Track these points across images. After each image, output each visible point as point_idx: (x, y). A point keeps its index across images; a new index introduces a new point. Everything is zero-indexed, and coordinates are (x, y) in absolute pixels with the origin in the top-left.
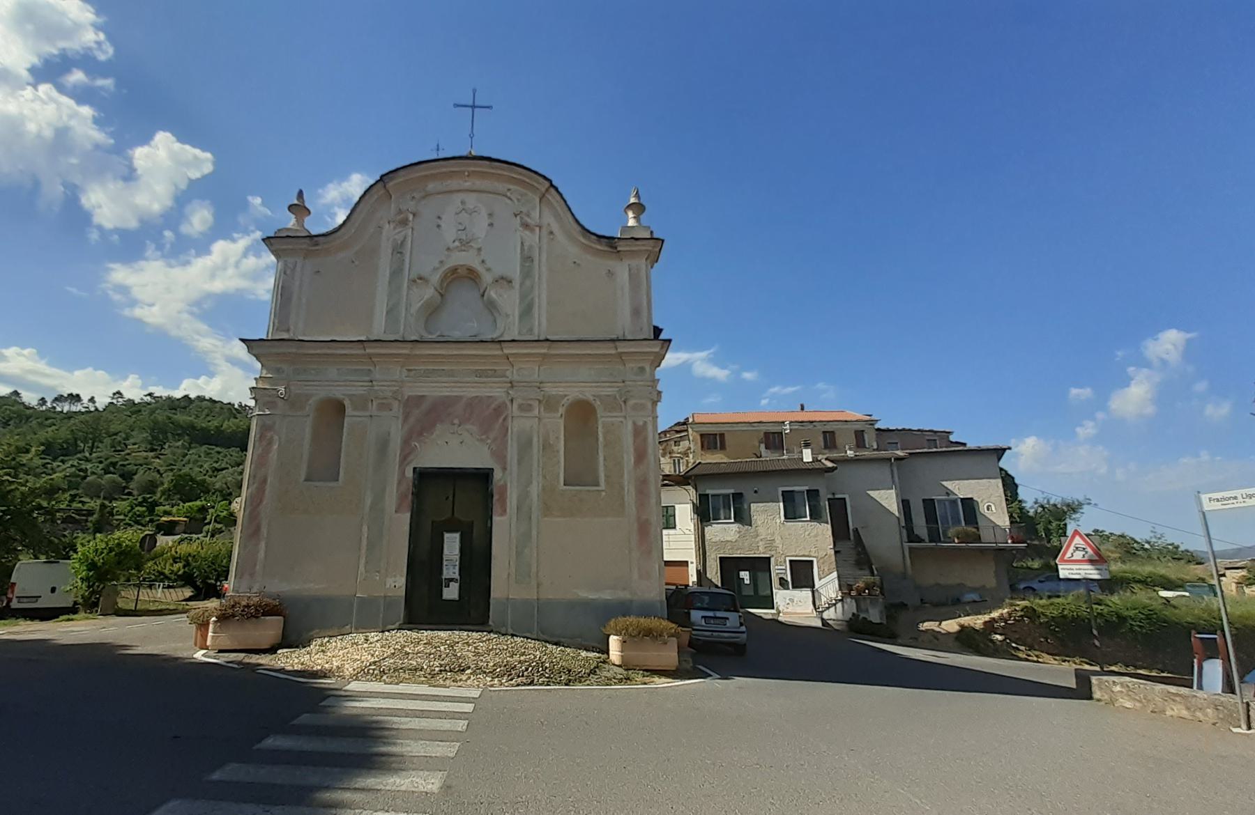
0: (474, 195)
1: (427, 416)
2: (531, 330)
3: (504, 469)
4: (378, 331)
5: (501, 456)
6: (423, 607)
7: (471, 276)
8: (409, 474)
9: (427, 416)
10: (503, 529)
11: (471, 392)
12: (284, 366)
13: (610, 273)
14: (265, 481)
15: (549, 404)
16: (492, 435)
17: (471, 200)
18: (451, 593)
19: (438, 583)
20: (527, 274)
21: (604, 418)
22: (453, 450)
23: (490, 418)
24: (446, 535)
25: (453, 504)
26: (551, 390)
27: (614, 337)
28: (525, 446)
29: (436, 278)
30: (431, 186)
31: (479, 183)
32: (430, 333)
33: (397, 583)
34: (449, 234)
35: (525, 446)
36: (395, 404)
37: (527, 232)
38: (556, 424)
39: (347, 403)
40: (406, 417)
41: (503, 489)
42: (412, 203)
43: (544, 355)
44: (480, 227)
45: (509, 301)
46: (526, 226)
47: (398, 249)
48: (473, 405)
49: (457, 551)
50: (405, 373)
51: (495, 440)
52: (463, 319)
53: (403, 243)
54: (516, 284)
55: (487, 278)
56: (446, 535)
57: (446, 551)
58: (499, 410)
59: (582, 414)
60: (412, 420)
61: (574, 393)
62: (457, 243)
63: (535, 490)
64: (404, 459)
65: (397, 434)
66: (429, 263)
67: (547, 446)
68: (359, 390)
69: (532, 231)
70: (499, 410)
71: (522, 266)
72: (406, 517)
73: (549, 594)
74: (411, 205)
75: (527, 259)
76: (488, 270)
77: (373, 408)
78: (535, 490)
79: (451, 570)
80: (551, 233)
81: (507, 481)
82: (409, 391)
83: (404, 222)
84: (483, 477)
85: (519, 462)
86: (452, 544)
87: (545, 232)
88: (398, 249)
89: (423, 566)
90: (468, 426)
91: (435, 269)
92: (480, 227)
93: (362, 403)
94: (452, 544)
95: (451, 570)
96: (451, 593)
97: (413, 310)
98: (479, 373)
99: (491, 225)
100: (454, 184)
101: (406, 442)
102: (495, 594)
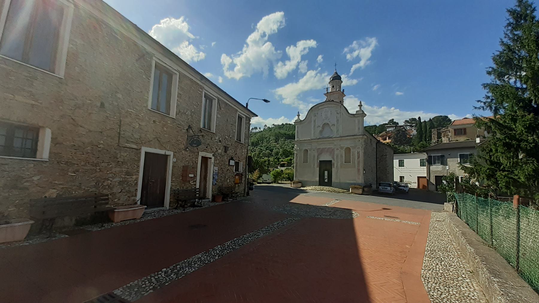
1: (321, 152)
4: (313, 138)
6: (322, 183)
7: (328, 124)
9: (321, 152)
10: (334, 170)
15: (342, 148)
18: (326, 181)
19: (324, 179)
20: (338, 123)
21: (352, 150)
22: (326, 157)
25: (326, 166)
26: (342, 146)
28: (337, 156)
30: (320, 108)
33: (318, 179)
35: (337, 156)
45: (334, 129)
47: (315, 121)
55: (330, 125)
58: (333, 150)
59: (348, 150)
61: (346, 146)
67: (341, 156)
68: (310, 148)
70: (333, 150)
72: (318, 169)
73: (342, 181)
75: (338, 120)
79: (326, 177)
84: (331, 161)
86: (326, 173)
88: (315, 121)
89: (321, 176)
94: (326, 173)
95: (326, 177)
96: (326, 181)
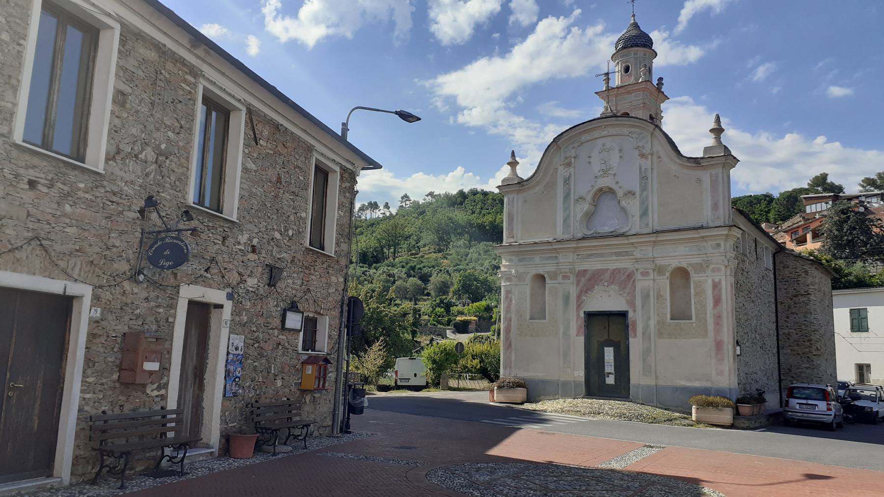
0: (610, 139)
1: (590, 281)
2: (647, 225)
3: (635, 311)
4: (560, 235)
5: (632, 303)
6: (595, 387)
7: (611, 191)
8: (582, 315)
9: (590, 281)
10: (635, 345)
11: (613, 266)
12: (514, 258)
13: (699, 181)
14: (510, 320)
15: (660, 270)
16: (627, 291)
17: (609, 142)
18: (610, 380)
19: (602, 375)
20: (644, 189)
21: (694, 277)
22: (606, 301)
23: (624, 280)
24: (606, 349)
25: (607, 330)
26: (660, 262)
27: (699, 225)
28: (646, 297)
29: (589, 197)
30: (584, 138)
31: (613, 131)
32: (590, 230)
33: (580, 374)
34: (596, 167)
35: (646, 297)
36: (571, 276)
37: (643, 160)
38: (664, 283)
39: (546, 276)
40: (578, 284)
41: (634, 324)
42: (573, 151)
43: (655, 242)
44: (614, 160)
45: (633, 206)
46: (642, 155)
47: (567, 181)
48: (615, 272)
49: (612, 358)
50: (576, 257)
51: (629, 293)
52: (607, 223)
53: (569, 178)
54: (638, 194)
55: (620, 193)
56: (606, 349)
57: (606, 358)
58: (630, 276)
59: (681, 275)
60: (581, 284)
61: (675, 263)
62: (601, 173)
63: (652, 323)
64: (579, 306)
65: (573, 291)
66: (584, 187)
67: (659, 297)
68: (552, 269)
69: (646, 158)
70: (630, 276)
71: (641, 183)
72: (582, 339)
73: (662, 382)
74: (572, 153)
75: (644, 178)
76: (621, 187)
77: (560, 278)
78: (652, 323)
79: (610, 368)
80: (659, 157)
81: (636, 317)
82: (580, 267)
83: (569, 164)
84: (623, 315)
85: (643, 307)
86: (609, 353)
87: (655, 157)
88: (567, 181)
89: (594, 364)
90: (613, 287)
91: (589, 192)
92: (614, 160)
93: (554, 276)
94: (609, 353)
95: (610, 368)
96: (610, 380)
97: (578, 218)
98: (618, 254)
99: (621, 157)
100: (596, 134)
101: (579, 297)
102: (632, 382)
